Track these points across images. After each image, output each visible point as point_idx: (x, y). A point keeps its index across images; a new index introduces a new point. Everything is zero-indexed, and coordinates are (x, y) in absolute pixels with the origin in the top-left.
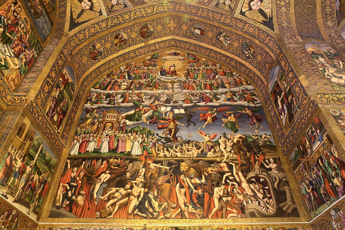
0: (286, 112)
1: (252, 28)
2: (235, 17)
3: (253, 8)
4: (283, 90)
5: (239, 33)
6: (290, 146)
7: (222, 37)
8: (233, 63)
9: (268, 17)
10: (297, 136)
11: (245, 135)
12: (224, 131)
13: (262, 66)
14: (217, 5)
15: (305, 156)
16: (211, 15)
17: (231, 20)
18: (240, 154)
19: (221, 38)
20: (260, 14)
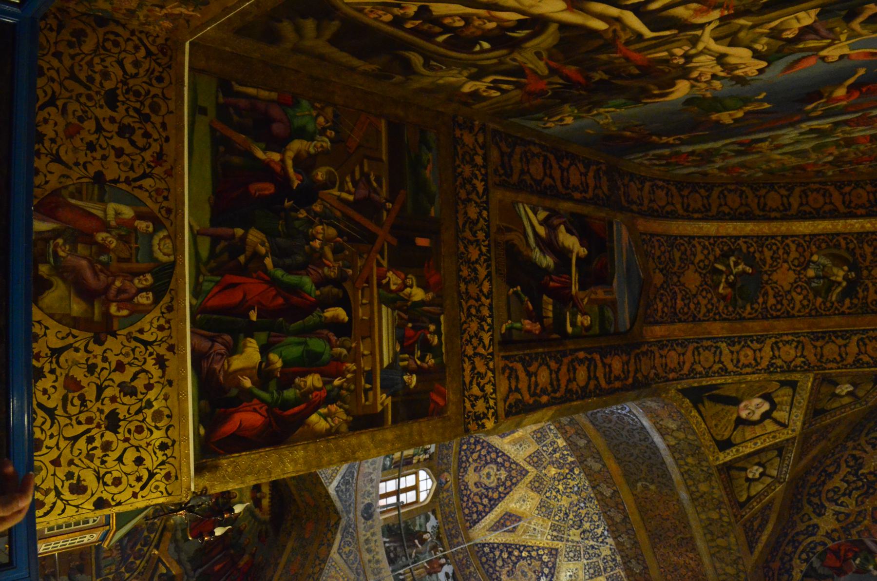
0: (537, 255)
1: (747, 362)
2: (809, 371)
4: (581, 295)
5: (782, 325)
6: (460, 180)
7: (839, 279)
8: (773, 200)
9: (707, 403)
10: (462, 249)
11: (646, 103)
12: (747, 88)
13: (672, 260)
15: (394, 242)
17: (822, 356)
18: (638, 67)
19: (841, 273)
20: (734, 395)
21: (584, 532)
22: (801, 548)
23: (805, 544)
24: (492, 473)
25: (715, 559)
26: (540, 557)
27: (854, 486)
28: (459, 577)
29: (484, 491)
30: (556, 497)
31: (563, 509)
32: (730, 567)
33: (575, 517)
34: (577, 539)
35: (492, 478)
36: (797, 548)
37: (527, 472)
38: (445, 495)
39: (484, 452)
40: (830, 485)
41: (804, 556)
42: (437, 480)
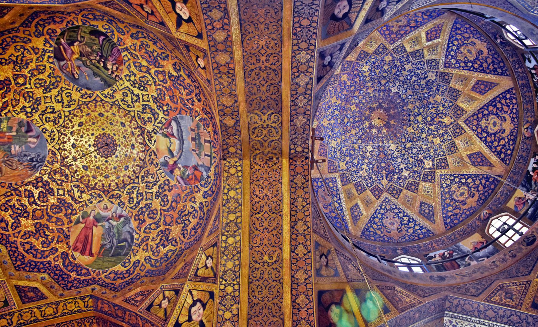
3: (194, 317)
14: (148, 309)
16: (141, 324)
21: (425, 78)
22: (210, 186)
23: (209, 188)
24: (491, 125)
25: (240, 201)
26: (458, 62)
27: (187, 217)
28: (521, 58)
29: (500, 114)
30: (445, 102)
31: (440, 93)
32: (232, 196)
33: (431, 88)
34: (430, 74)
35: (492, 122)
36: (212, 187)
37: (465, 122)
38: (529, 119)
39: (496, 144)
40: (196, 220)
41: (209, 180)
42: (533, 133)
